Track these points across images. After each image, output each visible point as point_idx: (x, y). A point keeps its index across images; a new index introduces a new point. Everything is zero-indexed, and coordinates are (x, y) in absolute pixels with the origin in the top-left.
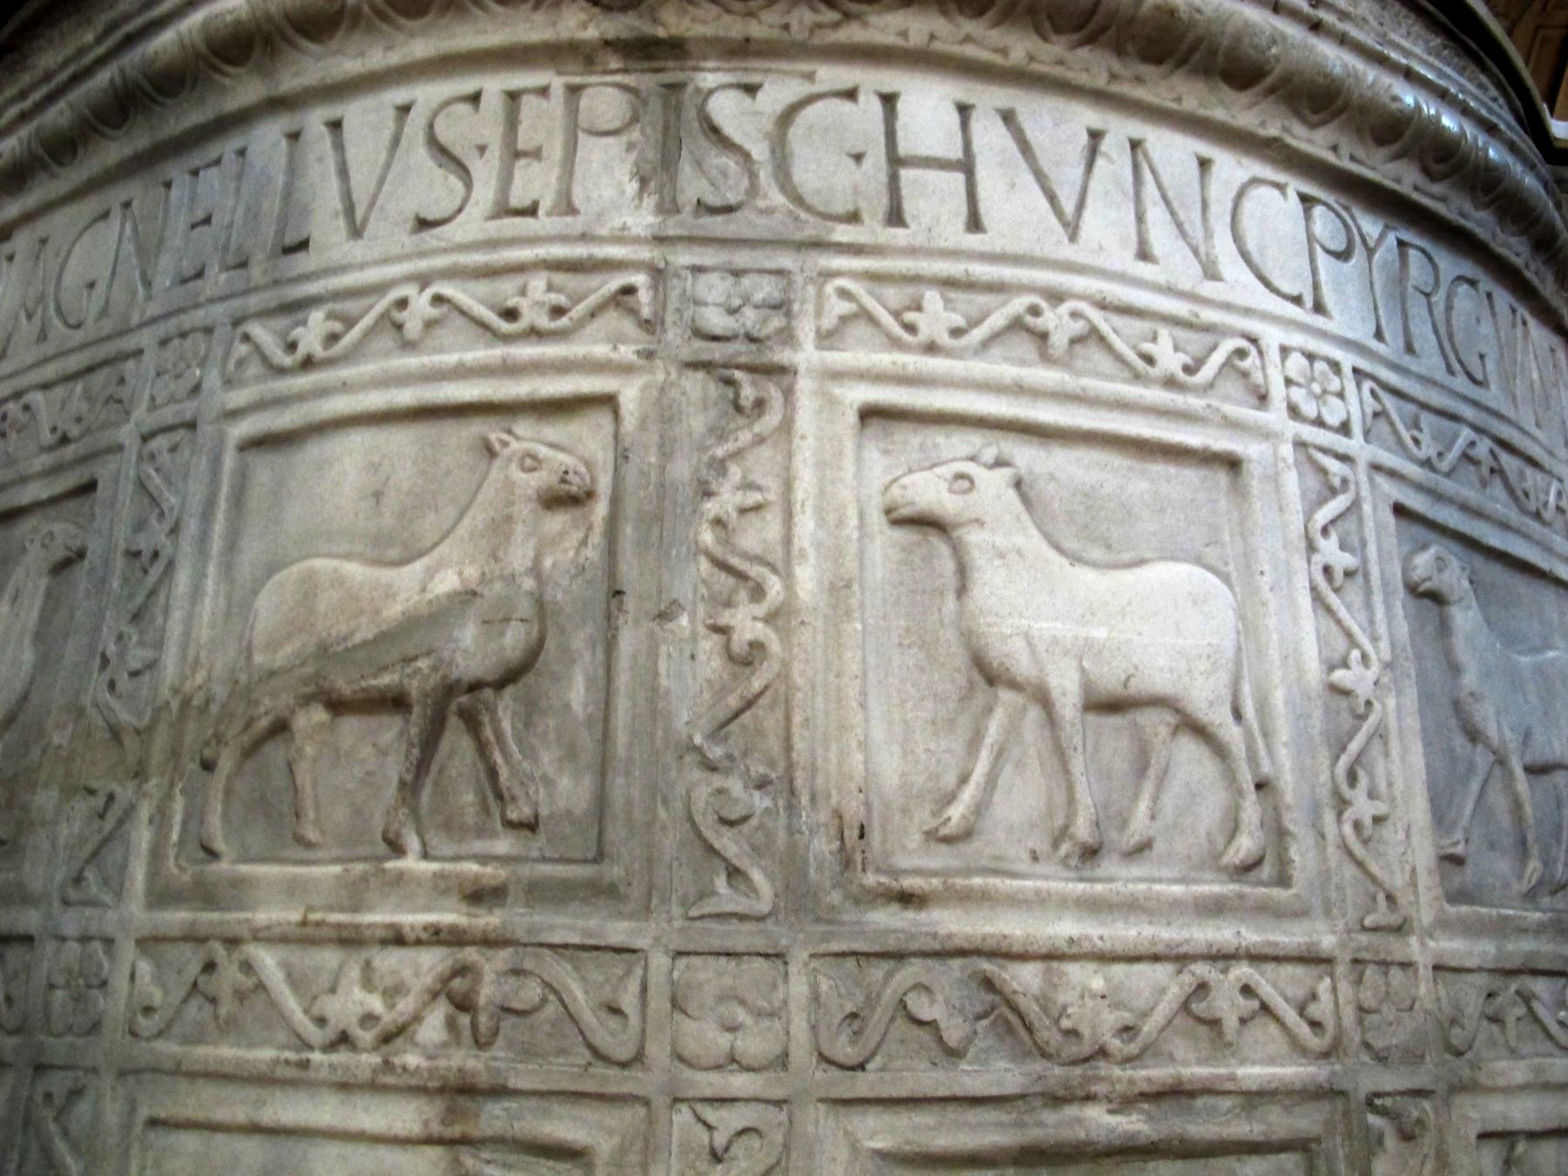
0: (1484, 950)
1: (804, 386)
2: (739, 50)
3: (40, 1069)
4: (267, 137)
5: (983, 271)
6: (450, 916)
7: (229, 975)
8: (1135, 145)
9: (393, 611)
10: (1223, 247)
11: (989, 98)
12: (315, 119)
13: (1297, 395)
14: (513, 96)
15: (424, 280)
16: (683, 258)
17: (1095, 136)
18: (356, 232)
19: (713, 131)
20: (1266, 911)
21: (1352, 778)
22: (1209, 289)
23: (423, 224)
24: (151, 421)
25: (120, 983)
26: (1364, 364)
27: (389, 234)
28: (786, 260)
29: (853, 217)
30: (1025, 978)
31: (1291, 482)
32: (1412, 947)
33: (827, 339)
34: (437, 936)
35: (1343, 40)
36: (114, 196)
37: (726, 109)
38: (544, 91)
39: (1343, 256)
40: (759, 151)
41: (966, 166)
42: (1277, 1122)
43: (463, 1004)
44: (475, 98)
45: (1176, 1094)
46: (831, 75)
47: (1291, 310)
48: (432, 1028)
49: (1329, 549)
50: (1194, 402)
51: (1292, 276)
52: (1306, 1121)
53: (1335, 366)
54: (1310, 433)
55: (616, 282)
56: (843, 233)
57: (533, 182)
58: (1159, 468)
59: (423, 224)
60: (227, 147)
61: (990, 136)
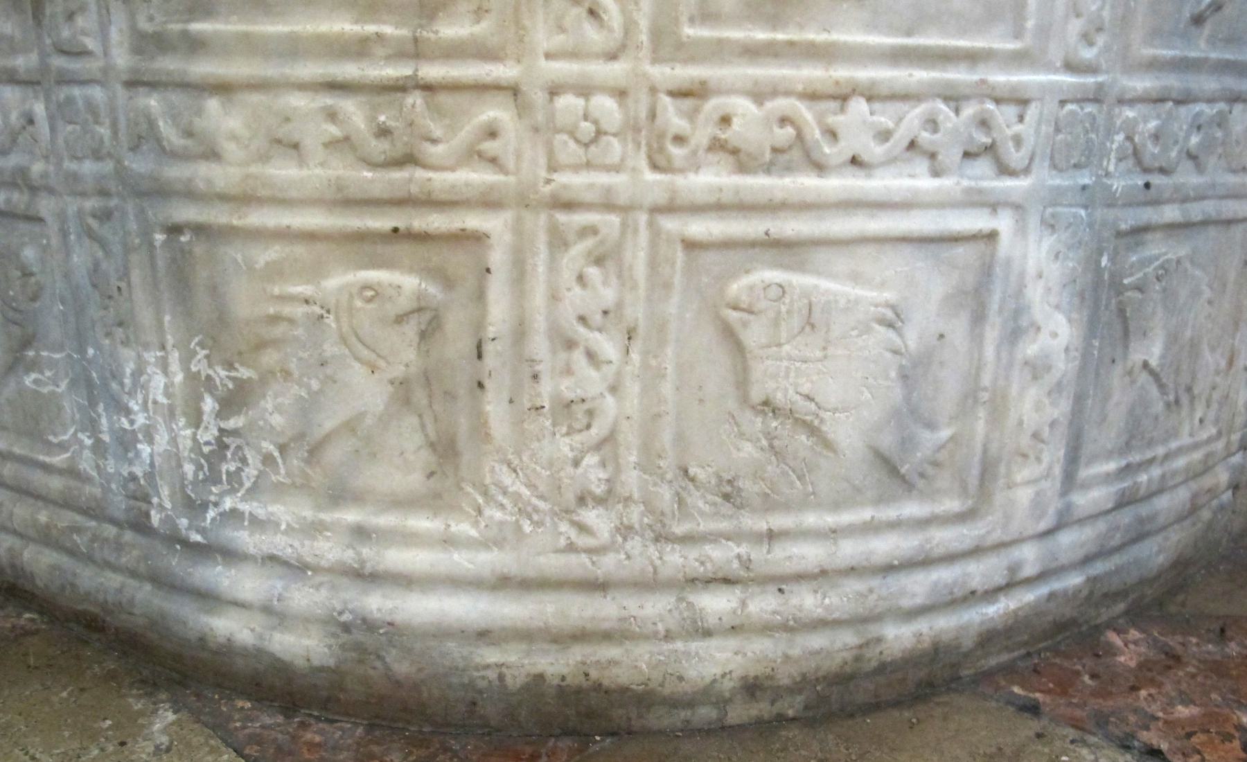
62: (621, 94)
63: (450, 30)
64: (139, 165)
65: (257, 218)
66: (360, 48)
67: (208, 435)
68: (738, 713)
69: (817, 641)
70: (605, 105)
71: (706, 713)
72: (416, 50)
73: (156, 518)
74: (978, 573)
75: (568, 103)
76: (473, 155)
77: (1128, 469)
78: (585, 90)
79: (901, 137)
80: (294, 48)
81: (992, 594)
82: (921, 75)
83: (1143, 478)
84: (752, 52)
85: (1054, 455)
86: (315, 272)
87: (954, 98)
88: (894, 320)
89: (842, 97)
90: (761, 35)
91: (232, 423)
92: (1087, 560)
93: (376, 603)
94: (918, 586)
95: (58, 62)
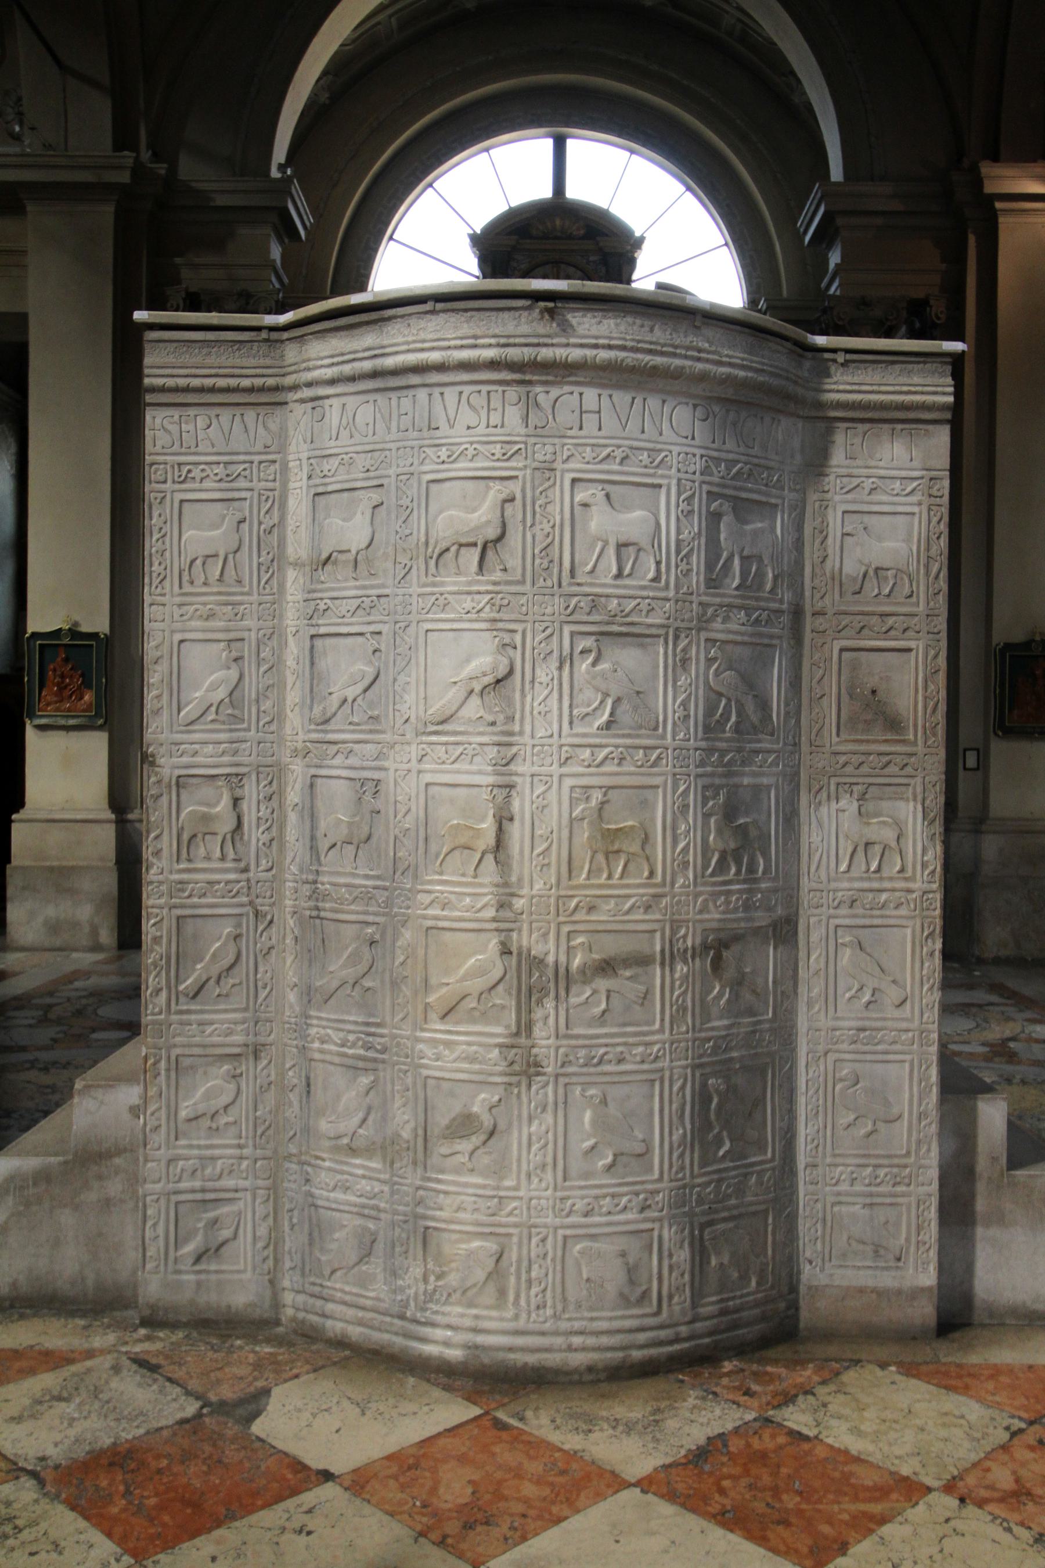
2: (546, 383)
4: (422, 394)
6: (490, 588)
7: (441, 601)
9: (472, 525)
10: (666, 425)
11: (605, 393)
12: (436, 391)
14: (489, 392)
15: (472, 443)
16: (532, 440)
17: (634, 399)
18: (452, 427)
22: (661, 439)
23: (469, 428)
24: (400, 470)
25: (415, 603)
26: (703, 452)
27: (460, 428)
28: (556, 441)
32: (694, 597)
34: (488, 592)
35: (707, 361)
36: (371, 397)
37: (541, 398)
39: (704, 420)
41: (599, 412)
46: (567, 388)
47: (684, 441)
48: (487, 609)
53: (694, 455)
54: (682, 475)
55: (517, 447)
56: (570, 433)
57: (495, 419)
58: (642, 489)
60: (411, 393)
61: (605, 401)
63: (508, 1183)
64: (420, 1210)
65: (453, 1227)
66: (484, 1187)
67: (430, 1287)
68: (587, 1377)
69: (609, 1355)
70: (543, 1202)
71: (576, 1377)
72: (498, 1188)
73: (408, 1314)
76: (510, 1214)
78: (539, 1198)
80: (466, 1185)
81: (671, 1342)
82: (625, 1189)
83: (731, 1303)
84: (581, 1188)
86: (469, 1241)
87: (637, 1194)
89: (605, 1196)
90: (583, 1183)
91: (440, 1283)
92: (710, 1334)
93: (480, 1339)
94: (642, 1337)
95: (396, 1179)
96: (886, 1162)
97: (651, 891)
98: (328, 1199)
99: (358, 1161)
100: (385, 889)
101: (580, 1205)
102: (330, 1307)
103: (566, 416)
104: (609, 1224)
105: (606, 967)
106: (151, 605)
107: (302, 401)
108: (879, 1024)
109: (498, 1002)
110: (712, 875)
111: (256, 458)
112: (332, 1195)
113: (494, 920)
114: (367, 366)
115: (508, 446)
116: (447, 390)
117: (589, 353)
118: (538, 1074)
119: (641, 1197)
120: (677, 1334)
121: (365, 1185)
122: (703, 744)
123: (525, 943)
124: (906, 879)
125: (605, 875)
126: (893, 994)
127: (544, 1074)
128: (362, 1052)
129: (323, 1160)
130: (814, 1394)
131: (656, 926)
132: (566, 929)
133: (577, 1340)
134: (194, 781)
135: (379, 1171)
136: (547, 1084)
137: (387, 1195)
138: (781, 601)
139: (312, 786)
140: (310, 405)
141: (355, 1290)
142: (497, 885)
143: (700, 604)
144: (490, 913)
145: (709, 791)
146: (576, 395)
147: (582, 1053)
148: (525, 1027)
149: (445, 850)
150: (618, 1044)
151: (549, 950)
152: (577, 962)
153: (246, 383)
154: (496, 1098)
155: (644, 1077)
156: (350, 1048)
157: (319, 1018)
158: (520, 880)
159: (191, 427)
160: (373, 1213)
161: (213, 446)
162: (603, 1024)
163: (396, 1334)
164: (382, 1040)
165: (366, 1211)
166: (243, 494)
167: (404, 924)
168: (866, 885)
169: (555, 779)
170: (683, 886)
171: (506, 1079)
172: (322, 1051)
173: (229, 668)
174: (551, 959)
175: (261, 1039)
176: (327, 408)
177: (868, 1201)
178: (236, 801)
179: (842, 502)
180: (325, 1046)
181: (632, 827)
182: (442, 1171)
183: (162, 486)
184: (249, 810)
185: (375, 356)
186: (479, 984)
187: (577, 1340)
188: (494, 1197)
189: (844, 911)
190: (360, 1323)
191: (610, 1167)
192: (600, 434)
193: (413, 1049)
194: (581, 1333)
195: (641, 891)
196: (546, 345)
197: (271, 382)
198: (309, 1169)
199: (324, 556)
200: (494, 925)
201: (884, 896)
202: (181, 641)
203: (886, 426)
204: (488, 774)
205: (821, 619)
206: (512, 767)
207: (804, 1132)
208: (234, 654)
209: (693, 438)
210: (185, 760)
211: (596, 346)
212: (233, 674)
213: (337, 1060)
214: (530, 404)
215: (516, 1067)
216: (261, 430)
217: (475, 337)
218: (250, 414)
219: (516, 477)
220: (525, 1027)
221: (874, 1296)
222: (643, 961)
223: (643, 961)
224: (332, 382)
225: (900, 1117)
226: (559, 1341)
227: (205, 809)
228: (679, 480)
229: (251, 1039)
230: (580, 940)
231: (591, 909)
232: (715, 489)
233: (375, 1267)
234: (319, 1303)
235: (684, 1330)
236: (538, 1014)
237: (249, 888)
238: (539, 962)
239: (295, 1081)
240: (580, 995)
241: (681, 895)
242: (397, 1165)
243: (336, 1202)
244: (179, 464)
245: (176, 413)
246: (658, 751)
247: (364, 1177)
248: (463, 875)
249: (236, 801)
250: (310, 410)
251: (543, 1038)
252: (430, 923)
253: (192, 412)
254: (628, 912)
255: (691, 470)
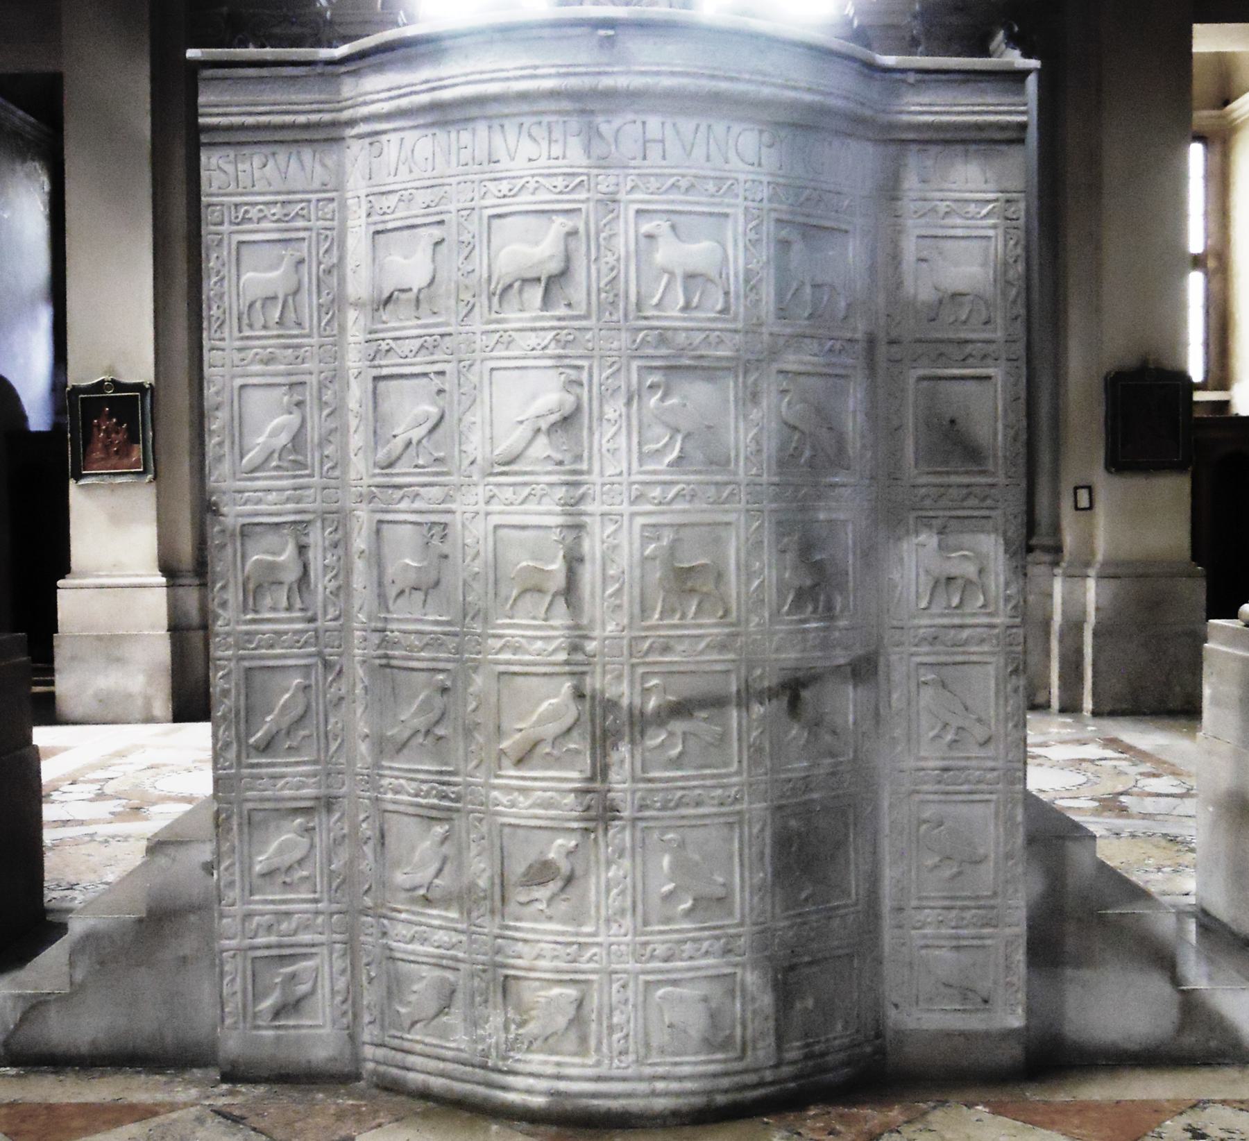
0: (788, 330)
1: (622, 205)
2: (606, 112)
3: (460, 361)
4: (481, 127)
5: (666, 171)
6: (555, 323)
7: (506, 338)
8: (709, 127)
10: (732, 155)
12: (496, 123)
13: (748, 194)
15: (533, 176)
16: (595, 171)
17: (698, 127)
19: (600, 135)
20: (725, 320)
21: (751, 289)
22: (727, 167)
23: (530, 160)
24: (461, 206)
25: (478, 341)
27: (521, 161)
29: (634, 158)
30: (670, 334)
31: (741, 219)
32: (764, 329)
33: (629, 192)
36: (430, 132)
37: (604, 128)
38: (557, 122)
39: (770, 146)
40: (612, 140)
41: (662, 141)
42: (724, 364)
43: (558, 341)
44: (540, 123)
45: (701, 357)
49: (752, 236)
50: (717, 200)
51: (751, 155)
52: (732, 364)
53: (761, 182)
56: (633, 163)
59: (530, 160)
62: (628, 945)
64: (499, 959)
66: (563, 933)
67: (511, 1036)
70: (623, 948)
72: (577, 934)
74: (751, 1078)
75: (614, 948)
76: (590, 960)
77: (807, 1045)
78: (619, 944)
79: (703, 950)
80: (545, 932)
82: (707, 933)
84: (661, 932)
85: (771, 1040)
87: (718, 938)
88: (705, 999)
89: (684, 942)
91: (521, 1031)
93: (562, 1086)
94: (725, 1082)
95: (474, 928)
96: (972, 903)
97: (727, 630)
98: (405, 952)
99: (434, 912)
100: (455, 635)
101: (661, 950)
102: (411, 1060)
103: (629, 146)
104: (689, 969)
105: (680, 709)
106: (212, 349)
107: (360, 137)
108: (964, 763)
109: (572, 746)
110: (788, 613)
111: (314, 197)
112: (410, 947)
113: (567, 663)
114: (425, 98)
115: (569, 179)
116: (506, 122)
117: (649, 81)
118: (614, 819)
119: (723, 941)
120: (762, 1078)
121: (442, 936)
122: (776, 479)
123: (598, 686)
124: (990, 615)
125: (678, 616)
126: (980, 732)
127: (620, 818)
128: (435, 801)
129: (400, 911)
130: (898, 1132)
131: (730, 666)
132: (640, 670)
133: (660, 1086)
134: (258, 529)
135: (457, 921)
136: (624, 828)
137: (465, 946)
138: (855, 330)
139: (378, 532)
140: (368, 140)
141: (435, 1041)
142: (569, 628)
143: (771, 334)
144: (562, 656)
145: (783, 527)
146: (639, 124)
147: (658, 797)
148: (600, 771)
149: (515, 593)
150: (695, 787)
151: (623, 692)
152: (652, 703)
153: (302, 119)
154: (573, 843)
155: (722, 820)
156: (425, 797)
157: (391, 768)
158: (592, 621)
159: (246, 166)
160: (451, 963)
161: (270, 184)
162: (679, 768)
163: (479, 1083)
164: (455, 789)
165: (444, 962)
166: (302, 234)
167: (475, 669)
168: (945, 621)
169: (626, 518)
170: (758, 625)
171: (582, 825)
172: (395, 802)
173: (291, 413)
174: (625, 702)
175: (334, 792)
176: (385, 143)
177: (954, 943)
178: (302, 549)
179: (916, 227)
180: (399, 797)
181: (704, 566)
182: (518, 919)
183: (220, 228)
184: (316, 558)
185: (433, 89)
186: (553, 729)
187: (660, 1086)
188: (572, 944)
189: (925, 648)
190: (442, 1074)
191: (688, 913)
192: (664, 163)
193: (487, 797)
194: (663, 1078)
195: (715, 631)
196: (606, 73)
197: (327, 117)
198: (385, 922)
199: (386, 294)
200: (567, 669)
201: (965, 634)
202: (242, 387)
203: (959, 148)
204: (558, 515)
205: (894, 348)
206: (582, 507)
207: (889, 875)
208: (297, 398)
209: (760, 165)
210: (249, 508)
211: (658, 73)
212: (294, 419)
213: (411, 810)
214: (591, 135)
215: (593, 813)
216: (318, 168)
217: (536, 67)
218: (307, 154)
219: (580, 210)
220: (600, 771)
221: (962, 1039)
222: (716, 702)
223: (716, 702)
224: (388, 116)
225: (986, 857)
226: (642, 1087)
227: (269, 558)
228: (746, 208)
229: (323, 791)
230: (654, 681)
231: (666, 649)
232: (785, 217)
233: (454, 1018)
234: (399, 1056)
235: (768, 1075)
236: (614, 757)
237: (317, 637)
238: (611, 705)
239: (369, 833)
240: (656, 738)
241: (755, 633)
242: (475, 914)
243: (413, 953)
244: (236, 205)
245: (231, 152)
246: (730, 487)
247: (440, 928)
248: (534, 618)
249: (302, 549)
250: (367, 146)
251: (620, 783)
252: (502, 668)
253: (246, 151)
254: (702, 653)
255: (758, 198)
